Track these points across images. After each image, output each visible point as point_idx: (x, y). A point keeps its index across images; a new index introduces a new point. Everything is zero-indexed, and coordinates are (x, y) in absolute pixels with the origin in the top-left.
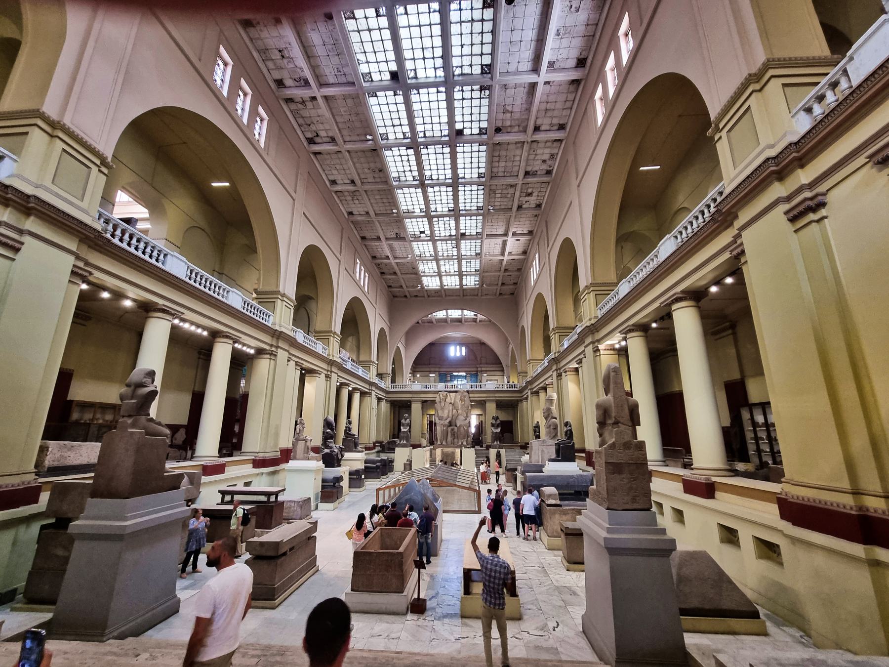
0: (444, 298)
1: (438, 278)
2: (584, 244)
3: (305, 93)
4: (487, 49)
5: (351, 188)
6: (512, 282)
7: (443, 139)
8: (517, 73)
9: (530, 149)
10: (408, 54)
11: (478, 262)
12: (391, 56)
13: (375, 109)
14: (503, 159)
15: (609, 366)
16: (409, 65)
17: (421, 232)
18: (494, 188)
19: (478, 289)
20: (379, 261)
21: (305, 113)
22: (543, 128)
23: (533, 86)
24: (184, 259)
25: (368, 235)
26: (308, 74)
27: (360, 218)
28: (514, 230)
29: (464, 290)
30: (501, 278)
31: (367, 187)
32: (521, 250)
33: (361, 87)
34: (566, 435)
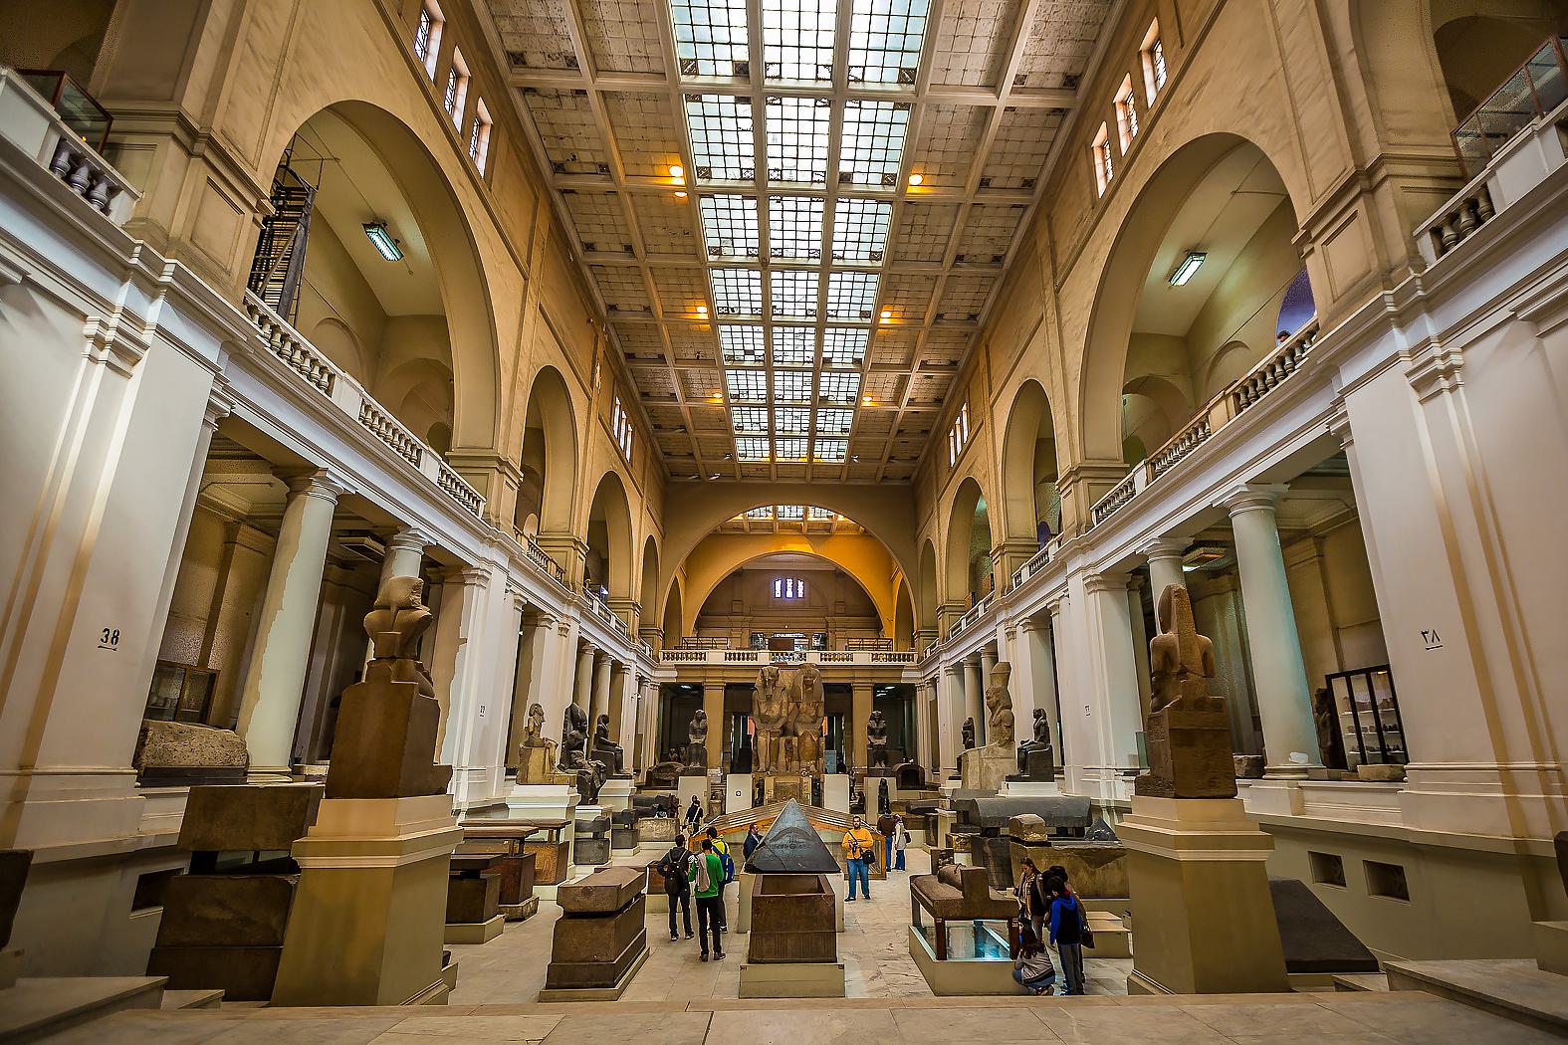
0: (773, 483)
1: (766, 444)
2: (1067, 399)
3: (566, 81)
4: (915, 43)
5: (624, 260)
6: (908, 456)
7: (816, 186)
8: (961, 88)
9: (969, 216)
10: (770, 37)
11: (849, 415)
12: (740, 35)
13: (695, 123)
14: (919, 230)
15: (1169, 588)
16: (770, 55)
17: (747, 352)
18: (896, 279)
19: (842, 466)
20: (653, 403)
21: (559, 117)
22: (993, 183)
23: (986, 112)
24: (359, 385)
25: (640, 352)
26: (576, 47)
27: (630, 318)
28: (924, 358)
29: (815, 466)
30: (889, 446)
31: (655, 261)
32: (931, 396)
33: (676, 82)
34: (1037, 732)
